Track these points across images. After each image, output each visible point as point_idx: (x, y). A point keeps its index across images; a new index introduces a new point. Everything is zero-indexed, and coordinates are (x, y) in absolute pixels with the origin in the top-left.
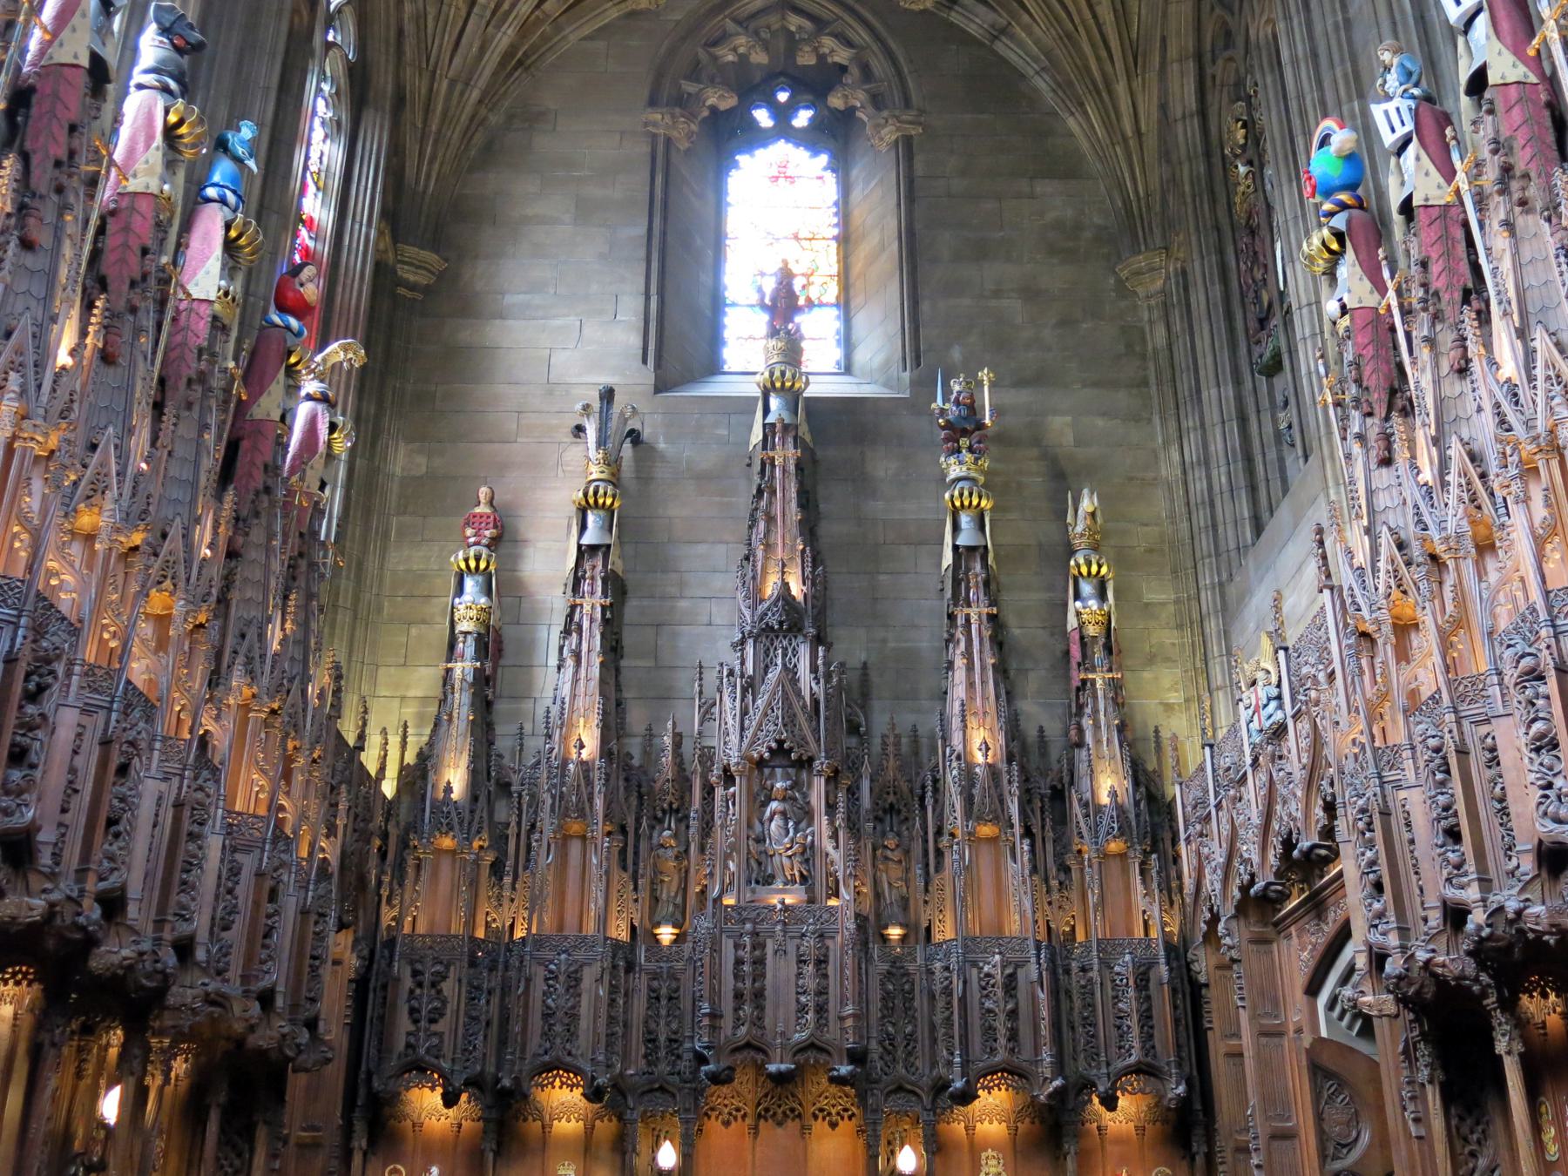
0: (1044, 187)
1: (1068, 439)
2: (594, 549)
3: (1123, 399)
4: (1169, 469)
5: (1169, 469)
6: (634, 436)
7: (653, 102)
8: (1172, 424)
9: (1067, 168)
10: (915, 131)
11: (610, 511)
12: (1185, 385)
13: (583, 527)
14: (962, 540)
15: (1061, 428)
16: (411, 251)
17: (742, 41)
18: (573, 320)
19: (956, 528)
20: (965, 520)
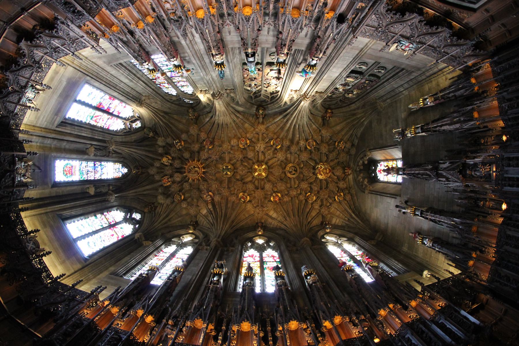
0: (373, 125)
1: (405, 113)
2: (421, 214)
3: (398, 105)
4: (406, 93)
5: (406, 93)
6: (406, 202)
7: (364, 192)
8: (400, 94)
9: (370, 123)
10: (368, 149)
11: (415, 209)
12: (393, 94)
13: (418, 215)
14: (419, 130)
15: (403, 115)
16: (376, 238)
17: (359, 178)
18: (390, 211)
19: (419, 133)
20: (417, 131)
